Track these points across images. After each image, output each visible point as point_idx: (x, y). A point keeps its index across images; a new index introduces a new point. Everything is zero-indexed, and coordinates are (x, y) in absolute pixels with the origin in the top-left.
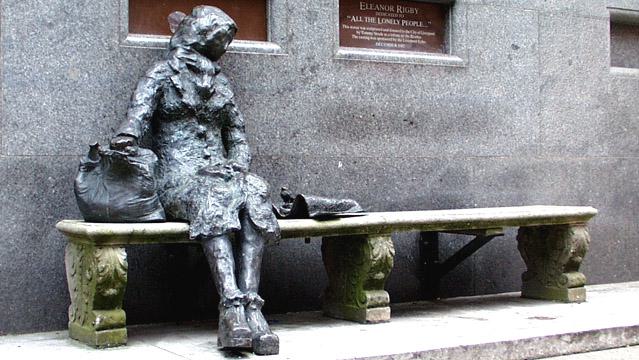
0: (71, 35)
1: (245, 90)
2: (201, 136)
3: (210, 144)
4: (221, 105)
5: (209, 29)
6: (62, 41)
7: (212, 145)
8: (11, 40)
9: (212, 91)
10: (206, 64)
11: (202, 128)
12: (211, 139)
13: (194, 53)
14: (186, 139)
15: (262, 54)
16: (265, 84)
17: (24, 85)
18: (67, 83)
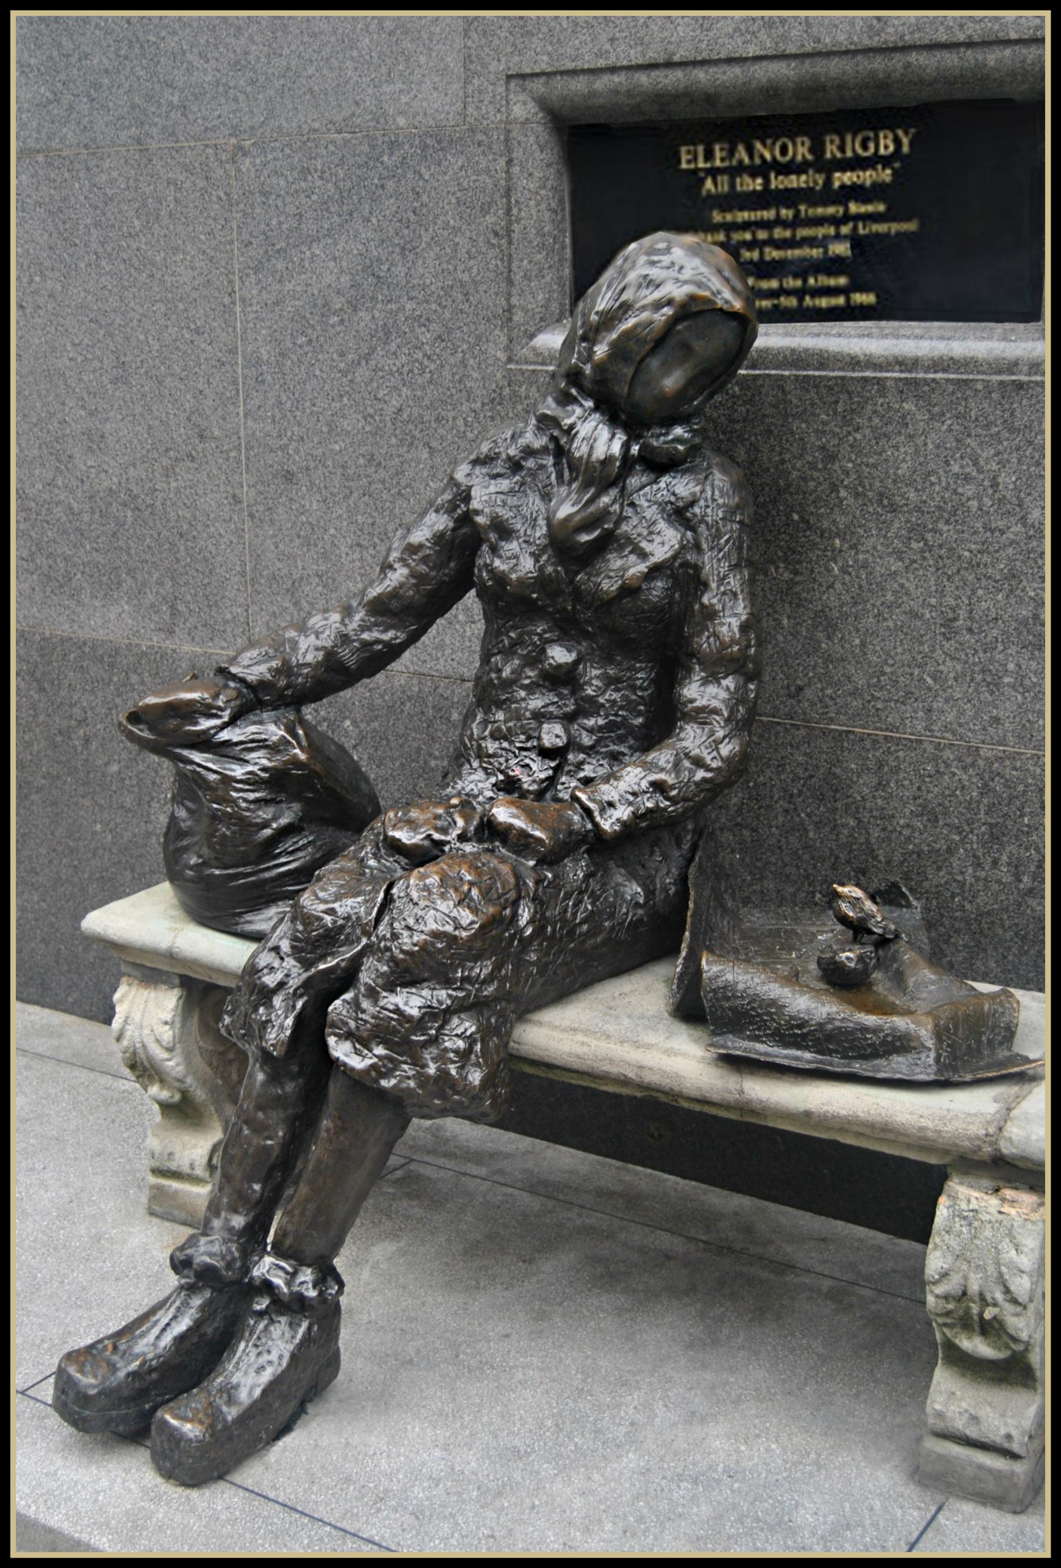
0: (388, 334)
1: (894, 509)
2: (562, 680)
3: (587, 707)
4: (609, 586)
5: (609, 319)
6: (367, 357)
7: (588, 715)
8: (259, 362)
9: (585, 538)
10: (598, 439)
11: (559, 655)
12: (590, 691)
13: (574, 400)
14: (508, 684)
15: (914, 380)
16: (969, 490)
17: (289, 477)
18: (382, 474)
